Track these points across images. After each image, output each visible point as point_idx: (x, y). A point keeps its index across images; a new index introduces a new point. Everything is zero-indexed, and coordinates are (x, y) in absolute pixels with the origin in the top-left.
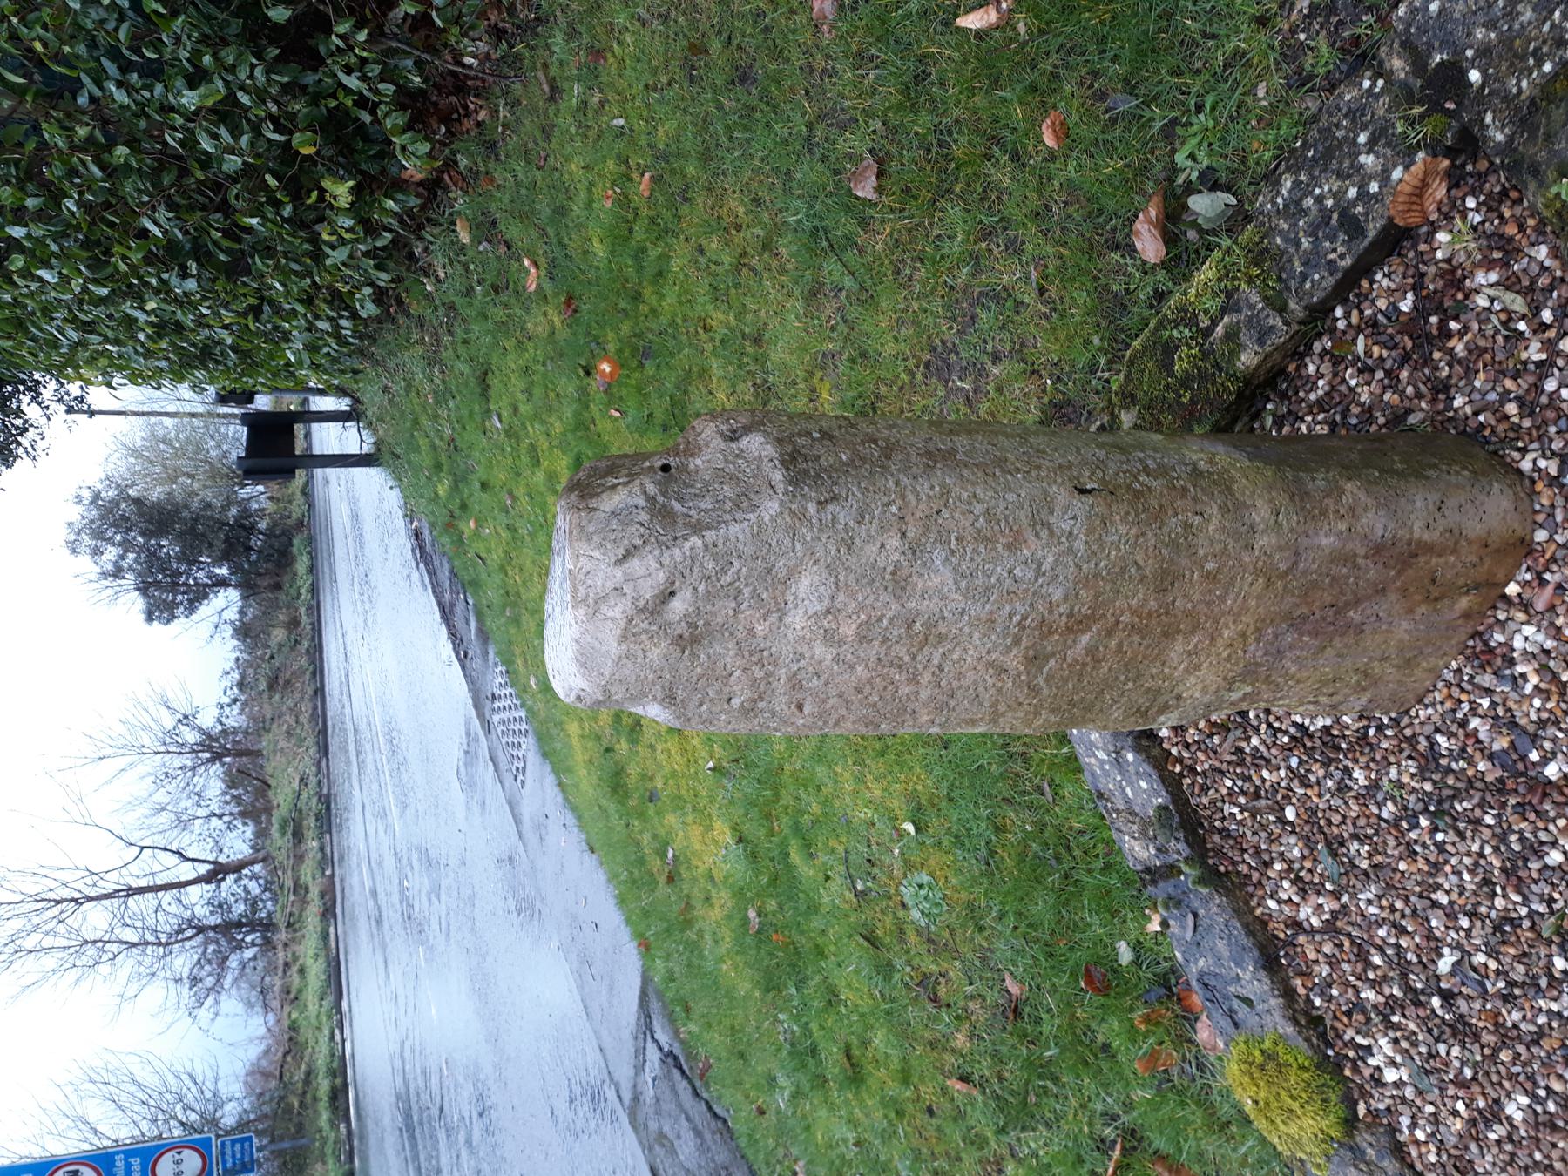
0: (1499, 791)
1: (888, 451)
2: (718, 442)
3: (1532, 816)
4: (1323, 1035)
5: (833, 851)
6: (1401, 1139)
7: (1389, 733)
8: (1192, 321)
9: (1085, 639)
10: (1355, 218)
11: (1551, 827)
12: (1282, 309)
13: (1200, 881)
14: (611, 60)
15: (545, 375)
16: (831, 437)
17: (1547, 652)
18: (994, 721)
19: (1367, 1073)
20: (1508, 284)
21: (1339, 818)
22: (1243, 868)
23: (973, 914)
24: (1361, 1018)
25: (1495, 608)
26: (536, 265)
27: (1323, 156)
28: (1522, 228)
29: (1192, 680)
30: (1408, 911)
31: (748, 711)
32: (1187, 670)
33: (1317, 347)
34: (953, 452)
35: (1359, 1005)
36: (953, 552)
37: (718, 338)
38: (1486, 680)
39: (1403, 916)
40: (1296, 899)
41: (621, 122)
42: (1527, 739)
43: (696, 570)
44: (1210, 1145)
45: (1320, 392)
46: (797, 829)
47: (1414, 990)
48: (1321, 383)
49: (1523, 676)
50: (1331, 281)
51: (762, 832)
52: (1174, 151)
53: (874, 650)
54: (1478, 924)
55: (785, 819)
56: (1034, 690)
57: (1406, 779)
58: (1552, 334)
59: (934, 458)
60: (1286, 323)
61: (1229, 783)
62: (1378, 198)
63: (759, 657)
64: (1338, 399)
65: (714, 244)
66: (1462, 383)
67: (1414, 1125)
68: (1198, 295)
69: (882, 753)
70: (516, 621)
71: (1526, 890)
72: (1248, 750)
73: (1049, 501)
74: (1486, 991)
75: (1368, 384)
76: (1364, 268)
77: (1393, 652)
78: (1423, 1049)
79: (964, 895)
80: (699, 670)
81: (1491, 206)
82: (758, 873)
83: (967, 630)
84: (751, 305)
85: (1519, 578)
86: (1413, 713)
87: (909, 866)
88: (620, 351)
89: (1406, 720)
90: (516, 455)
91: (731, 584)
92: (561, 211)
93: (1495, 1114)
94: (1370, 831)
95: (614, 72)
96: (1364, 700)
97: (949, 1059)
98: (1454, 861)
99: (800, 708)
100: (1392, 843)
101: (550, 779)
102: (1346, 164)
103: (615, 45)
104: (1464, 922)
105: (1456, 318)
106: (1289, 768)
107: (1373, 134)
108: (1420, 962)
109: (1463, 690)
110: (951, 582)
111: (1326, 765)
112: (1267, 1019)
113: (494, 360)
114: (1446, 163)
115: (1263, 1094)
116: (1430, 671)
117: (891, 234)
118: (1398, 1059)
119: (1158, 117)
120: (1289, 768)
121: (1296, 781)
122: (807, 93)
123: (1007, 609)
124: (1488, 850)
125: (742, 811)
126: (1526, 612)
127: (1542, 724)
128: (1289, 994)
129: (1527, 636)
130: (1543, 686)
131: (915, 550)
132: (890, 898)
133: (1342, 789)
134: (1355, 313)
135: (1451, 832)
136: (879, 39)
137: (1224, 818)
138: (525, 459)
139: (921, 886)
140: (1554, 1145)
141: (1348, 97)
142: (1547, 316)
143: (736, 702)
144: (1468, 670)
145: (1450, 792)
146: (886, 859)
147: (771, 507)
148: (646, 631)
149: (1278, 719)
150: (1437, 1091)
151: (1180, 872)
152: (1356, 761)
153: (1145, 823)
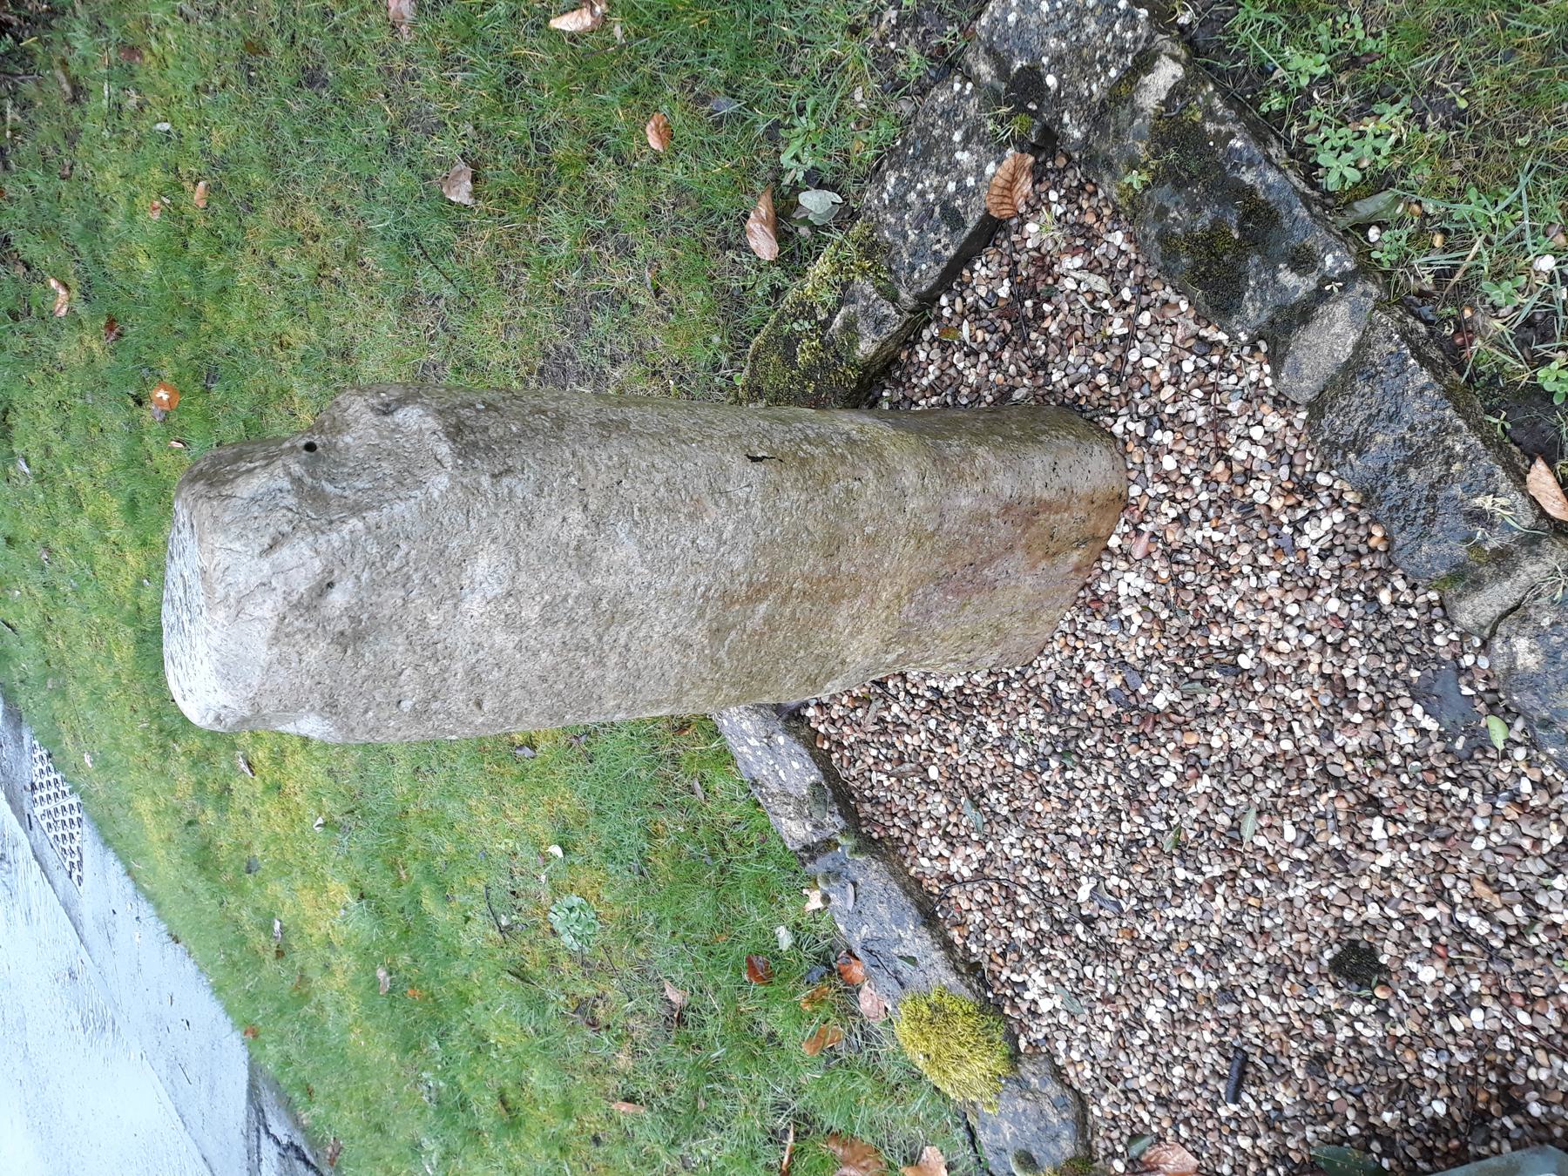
0: (1116, 725)
1: (560, 422)
2: (369, 417)
3: (1146, 744)
4: (982, 980)
5: (472, 890)
6: (1059, 1062)
7: (1016, 685)
8: (810, 314)
9: (762, 608)
10: (955, 211)
11: (1163, 751)
12: (894, 299)
13: (857, 850)
14: (149, 58)
15: (84, 409)
16: (497, 409)
17: (1146, 595)
18: (678, 701)
19: (1024, 1007)
20: (1090, 268)
21: (978, 771)
22: (895, 832)
23: (630, 931)
24: (1014, 956)
25: (1100, 560)
26: (66, 286)
27: (922, 153)
28: (1099, 218)
29: (856, 644)
30: (1047, 849)
31: (419, 714)
32: (851, 634)
33: (926, 334)
34: (625, 423)
35: (1010, 946)
36: (636, 524)
37: (298, 354)
38: (1097, 626)
39: (1043, 854)
40: (946, 853)
41: (167, 126)
42: (1136, 675)
43: (358, 556)
44: (881, 1111)
45: (932, 377)
46: (428, 873)
47: (1059, 922)
48: (931, 368)
49: (1128, 618)
50: (938, 270)
51: (387, 884)
52: (778, 153)
53: (557, 635)
54: (1109, 850)
55: (413, 866)
56: (716, 664)
57: (1034, 726)
58: (1131, 310)
59: (607, 428)
60: (900, 313)
61: (874, 752)
62: (975, 191)
63: (434, 651)
64: (948, 384)
65: (287, 257)
66: (1058, 359)
67: (1069, 1047)
68: (814, 289)
69: (521, 778)
70: (62, 693)
71: (1146, 812)
72: (889, 719)
73: (724, 469)
74: (1122, 910)
75: (975, 366)
76: (965, 258)
77: (1020, 605)
78: (1072, 975)
79: (618, 910)
80: (364, 671)
81: (1070, 198)
82: (385, 928)
83: (653, 605)
84: (335, 318)
85: (1119, 531)
86: (1035, 664)
87: (557, 891)
88: (178, 377)
89: (1030, 672)
90: (51, 502)
91: (399, 569)
92: (94, 227)
93: (1138, 1021)
94: (1007, 779)
95: (154, 72)
96: (995, 656)
97: (612, 1082)
98: (1083, 795)
99: (479, 705)
100: (1027, 788)
101: (118, 868)
102: (944, 160)
103: (154, 43)
104: (1097, 850)
105: (1048, 301)
106: (928, 730)
107: (966, 132)
108: (1062, 894)
109: (1077, 638)
110: (636, 555)
111: (962, 723)
112: (931, 973)
113: (16, 396)
114: (1031, 159)
115: (933, 1048)
116: (1049, 623)
117: (491, 240)
118: (1051, 988)
119: (762, 120)
120: (928, 730)
121: (936, 742)
122: (387, 96)
123: (692, 580)
124: (1111, 780)
125: (361, 866)
126: (1127, 561)
127: (1148, 660)
128: (948, 945)
129: (1130, 583)
130: (1145, 626)
131: (598, 523)
132: (538, 928)
133: (978, 743)
134: (959, 300)
135: (1078, 769)
136: (464, 42)
137: (872, 787)
138: (63, 506)
139: (571, 910)
140: (1189, 1038)
141: (941, 99)
142: (1126, 294)
143: (406, 705)
144: (1081, 619)
145: (1075, 733)
146: (532, 888)
147: (440, 483)
148: (301, 631)
149: (914, 685)
150: (1087, 1012)
151: (837, 845)
152: (989, 715)
153: (800, 802)
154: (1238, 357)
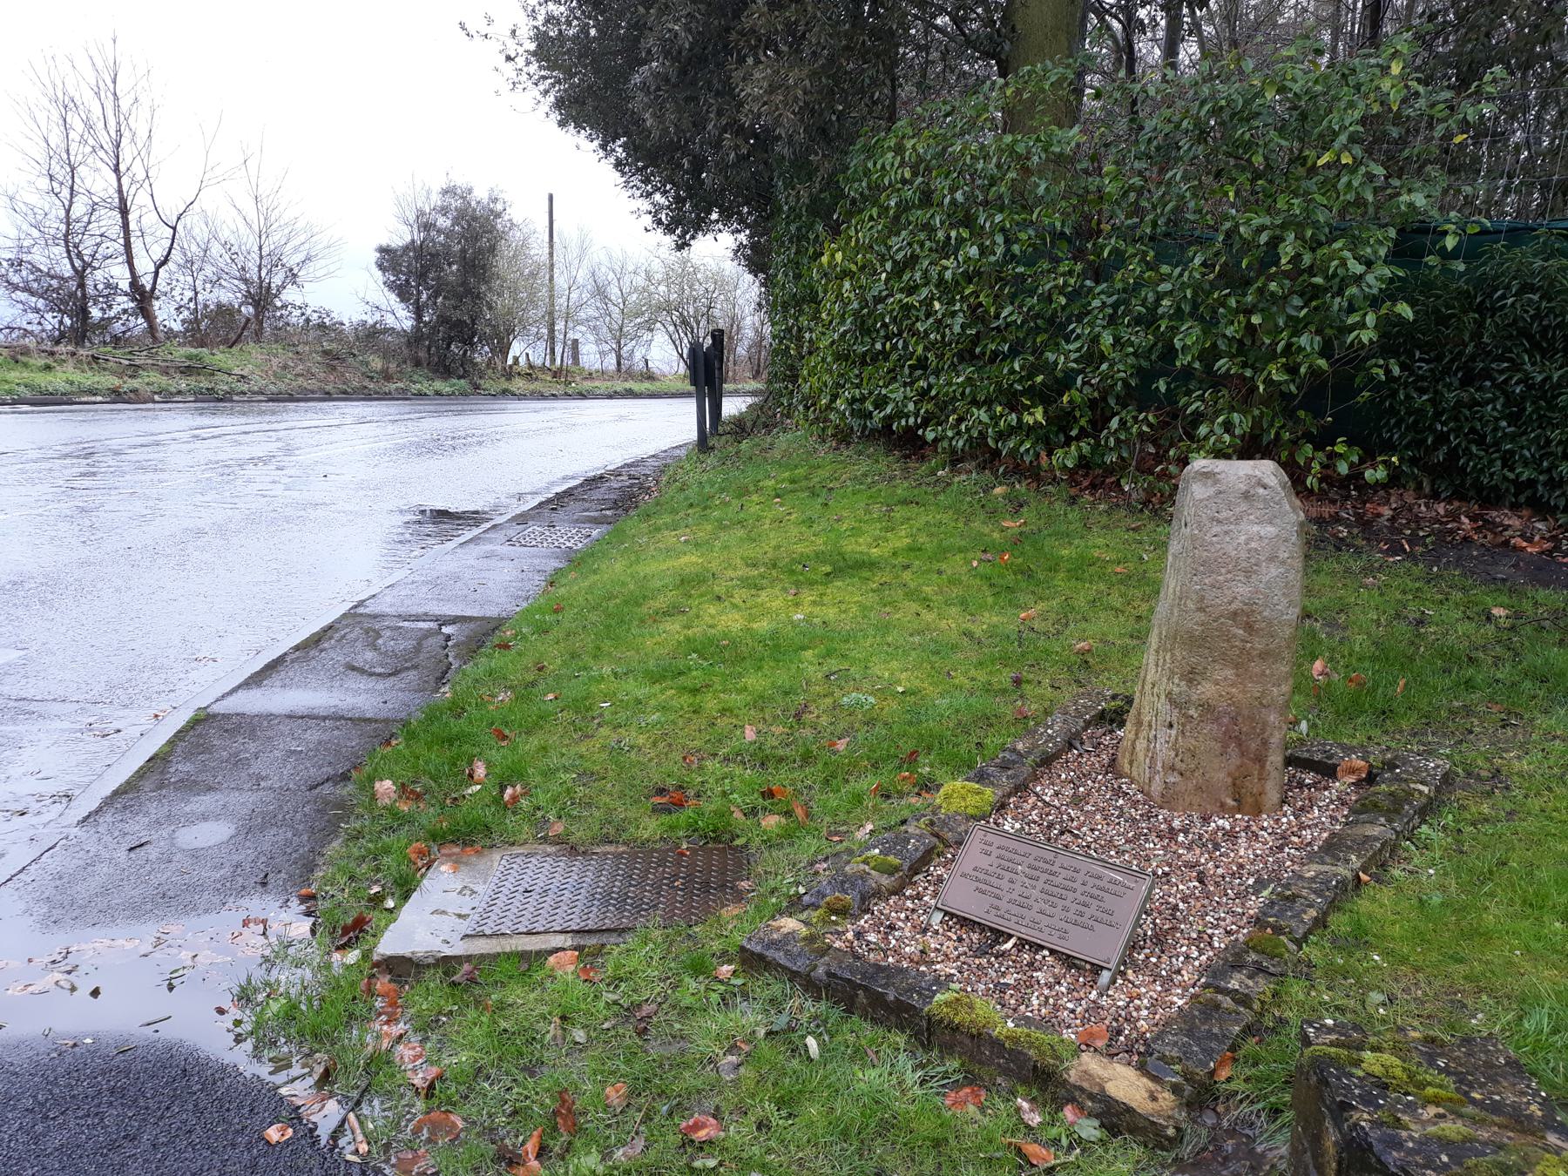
63: (1238, 520)
131: (1283, 563)
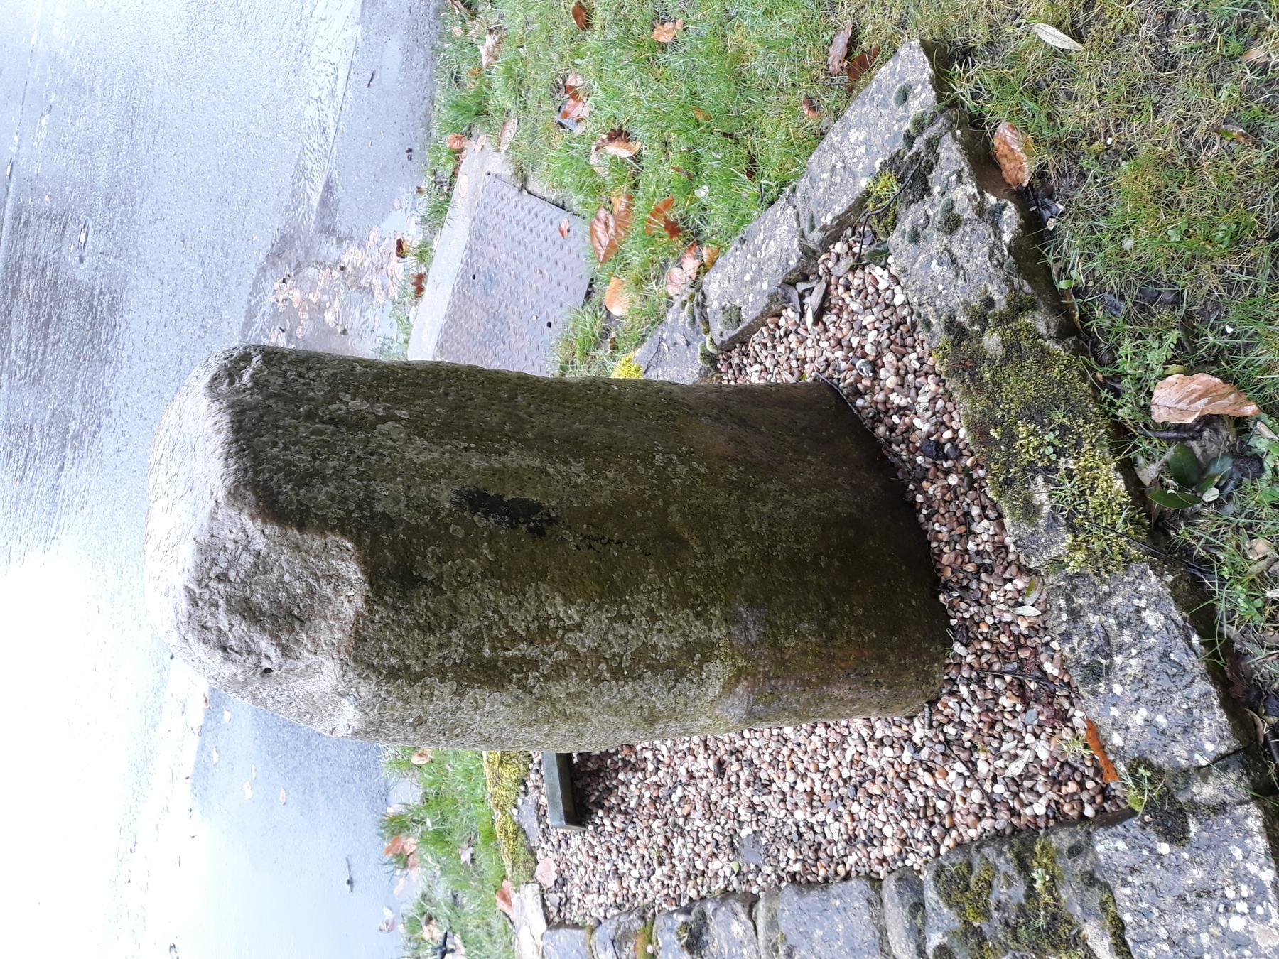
154: (928, 854)
